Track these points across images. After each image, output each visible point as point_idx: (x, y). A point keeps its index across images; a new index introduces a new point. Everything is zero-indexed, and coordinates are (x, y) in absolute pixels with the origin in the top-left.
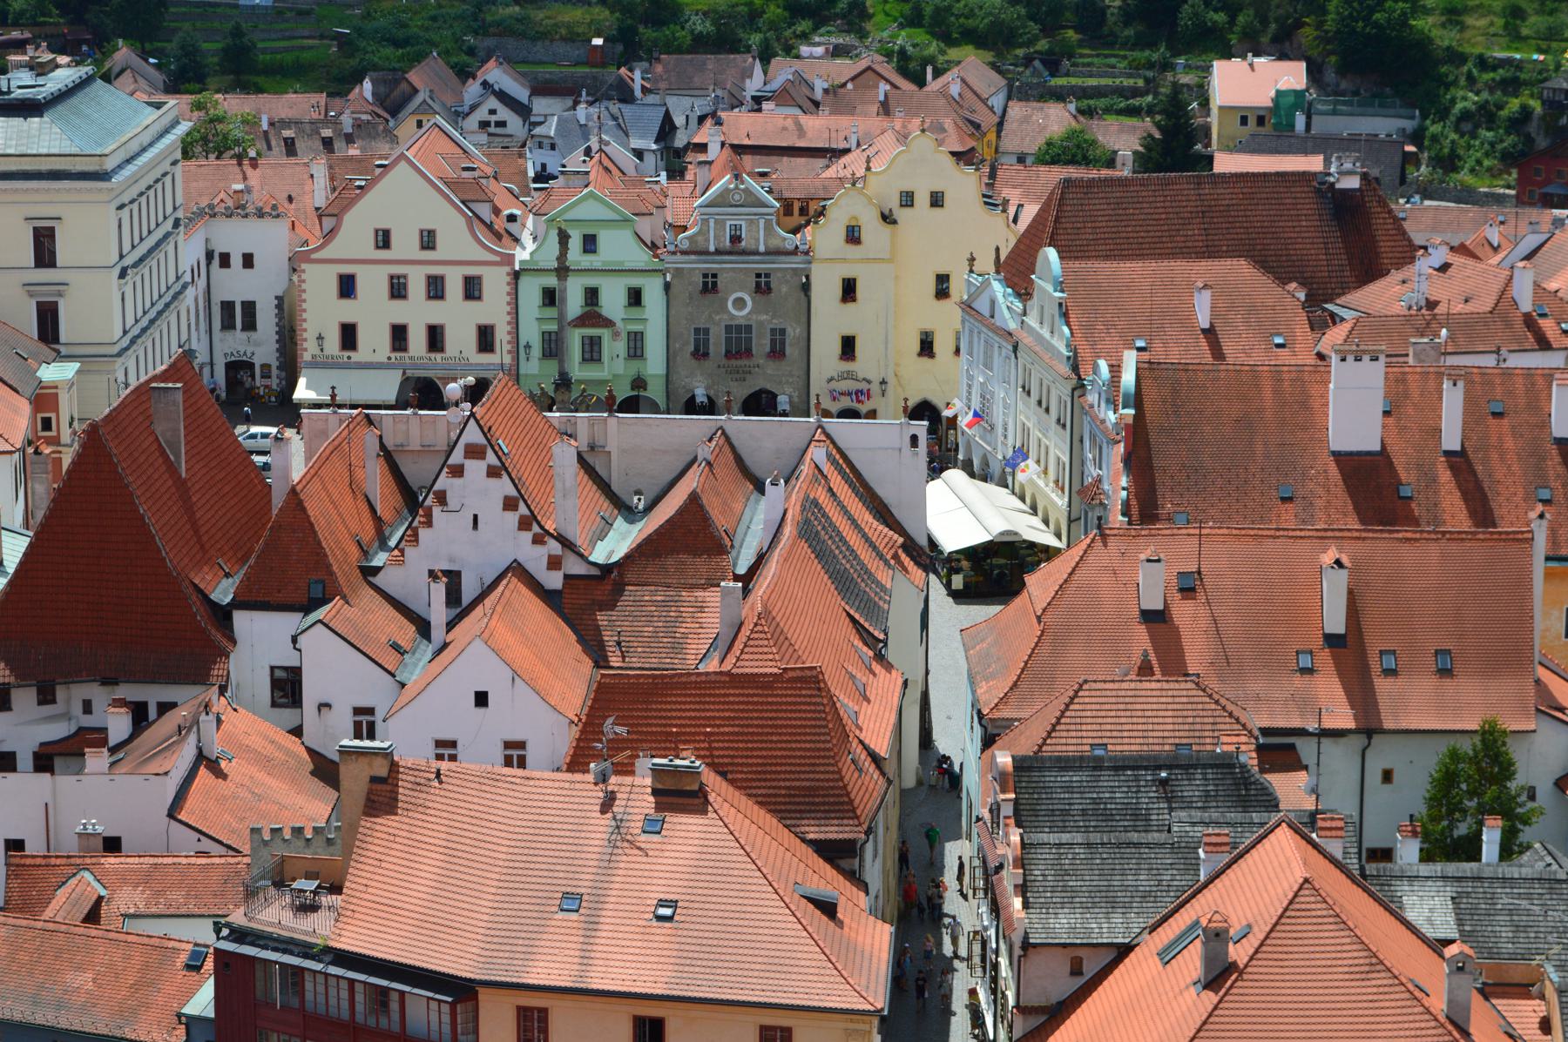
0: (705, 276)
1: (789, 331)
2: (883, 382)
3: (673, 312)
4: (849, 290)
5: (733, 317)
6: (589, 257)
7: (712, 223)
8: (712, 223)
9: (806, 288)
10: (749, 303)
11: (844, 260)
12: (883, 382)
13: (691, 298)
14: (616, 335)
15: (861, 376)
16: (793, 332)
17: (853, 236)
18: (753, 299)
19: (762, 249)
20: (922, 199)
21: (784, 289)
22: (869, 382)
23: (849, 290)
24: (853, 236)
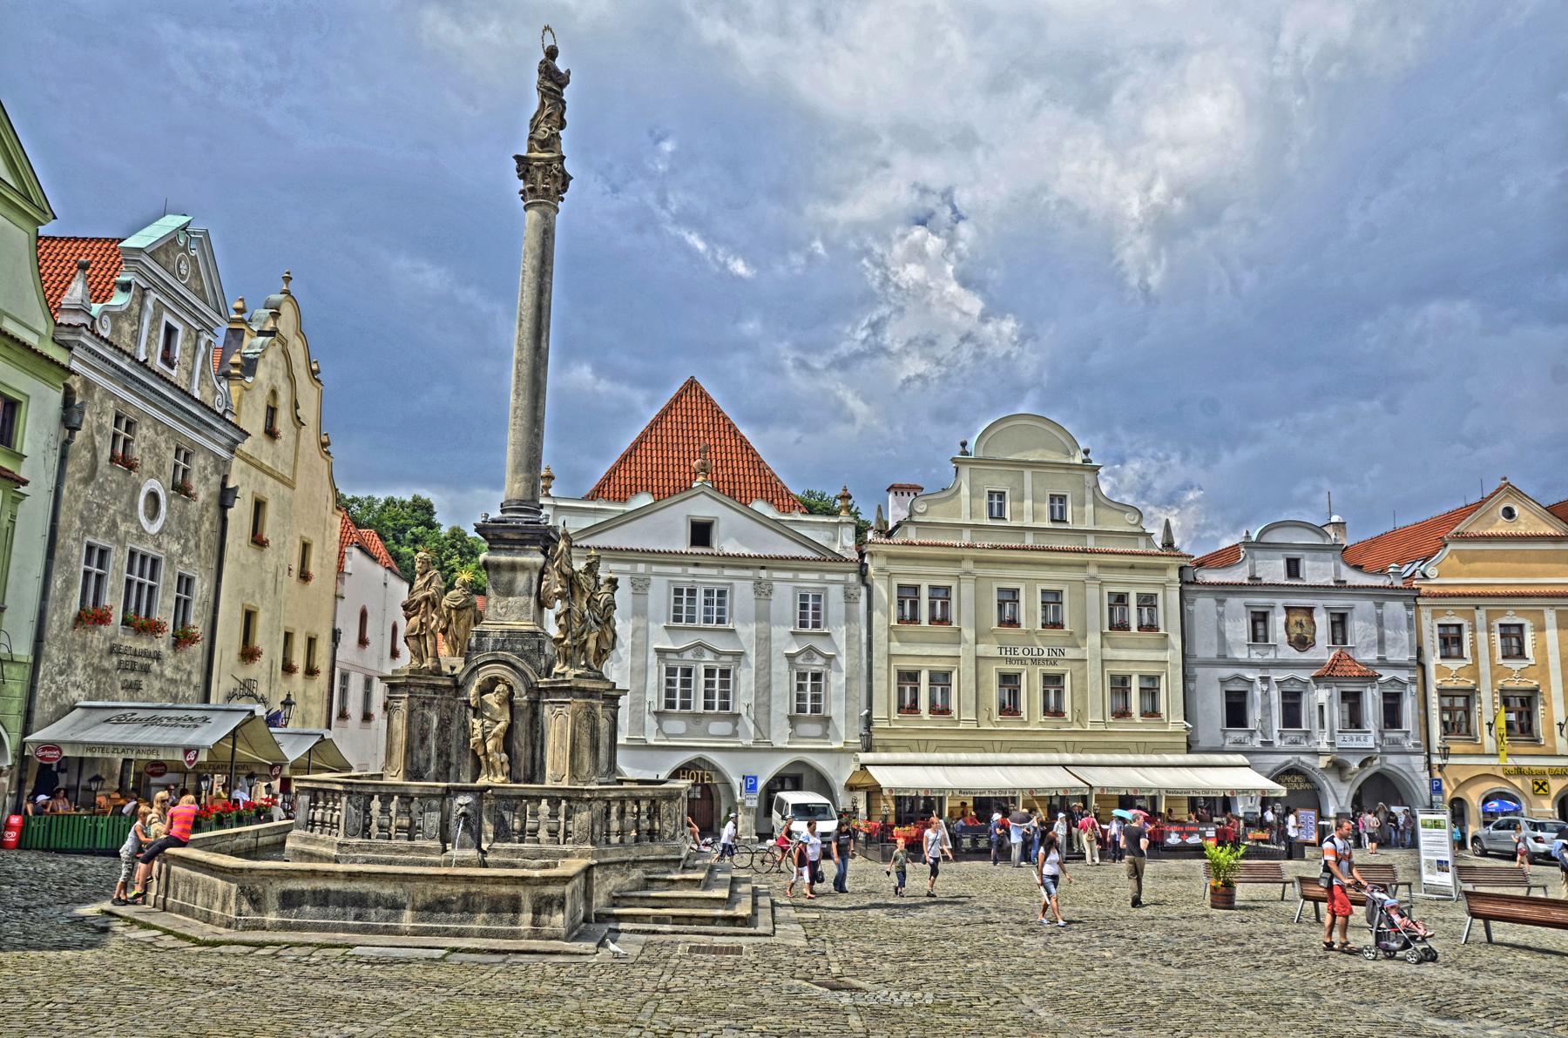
1: (197, 582)
5: (142, 535)
7: (149, 304)
9: (226, 497)
16: (202, 588)
19: (197, 395)
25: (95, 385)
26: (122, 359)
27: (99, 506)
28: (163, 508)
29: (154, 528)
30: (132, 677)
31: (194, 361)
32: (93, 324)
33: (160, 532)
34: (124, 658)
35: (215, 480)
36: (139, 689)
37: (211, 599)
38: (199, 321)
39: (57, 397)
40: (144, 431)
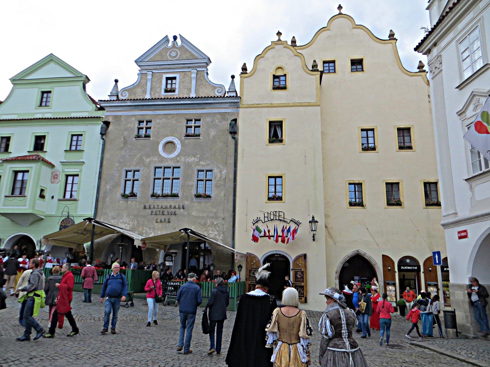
0: (140, 122)
2: (313, 221)
3: (107, 155)
4: (275, 131)
5: (162, 159)
6: (43, 110)
8: (149, 77)
10: (179, 146)
11: (272, 106)
12: (313, 221)
13: (125, 142)
14: (55, 177)
15: (288, 218)
17: (279, 83)
18: (183, 144)
19: (193, 95)
20: (343, 66)
21: (213, 133)
22: (298, 224)
23: (275, 131)
24: (279, 83)
25: (121, 116)
26: (126, 103)
27: (129, 156)
28: (179, 146)
29: (173, 155)
30: (163, 218)
31: (191, 84)
32: (118, 96)
33: (178, 156)
34: (154, 210)
35: (226, 125)
36: (169, 222)
37: (232, 176)
38: (189, 67)
39: (98, 127)
40: (158, 121)
